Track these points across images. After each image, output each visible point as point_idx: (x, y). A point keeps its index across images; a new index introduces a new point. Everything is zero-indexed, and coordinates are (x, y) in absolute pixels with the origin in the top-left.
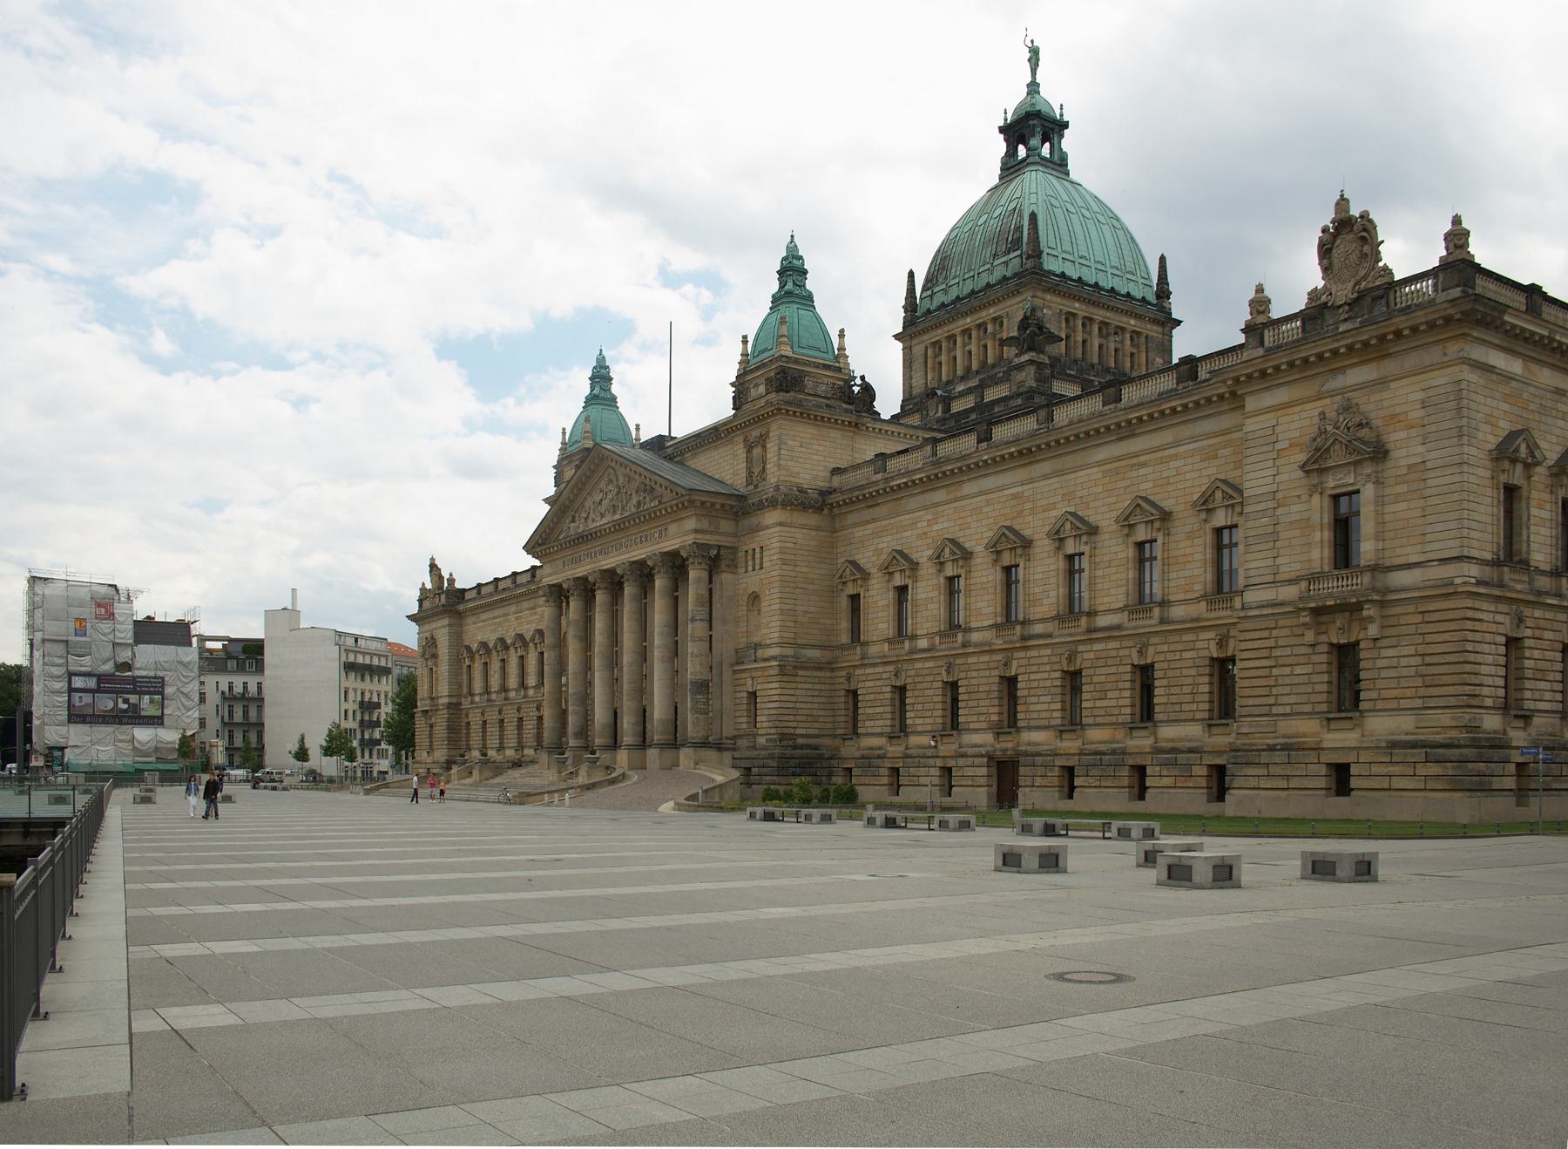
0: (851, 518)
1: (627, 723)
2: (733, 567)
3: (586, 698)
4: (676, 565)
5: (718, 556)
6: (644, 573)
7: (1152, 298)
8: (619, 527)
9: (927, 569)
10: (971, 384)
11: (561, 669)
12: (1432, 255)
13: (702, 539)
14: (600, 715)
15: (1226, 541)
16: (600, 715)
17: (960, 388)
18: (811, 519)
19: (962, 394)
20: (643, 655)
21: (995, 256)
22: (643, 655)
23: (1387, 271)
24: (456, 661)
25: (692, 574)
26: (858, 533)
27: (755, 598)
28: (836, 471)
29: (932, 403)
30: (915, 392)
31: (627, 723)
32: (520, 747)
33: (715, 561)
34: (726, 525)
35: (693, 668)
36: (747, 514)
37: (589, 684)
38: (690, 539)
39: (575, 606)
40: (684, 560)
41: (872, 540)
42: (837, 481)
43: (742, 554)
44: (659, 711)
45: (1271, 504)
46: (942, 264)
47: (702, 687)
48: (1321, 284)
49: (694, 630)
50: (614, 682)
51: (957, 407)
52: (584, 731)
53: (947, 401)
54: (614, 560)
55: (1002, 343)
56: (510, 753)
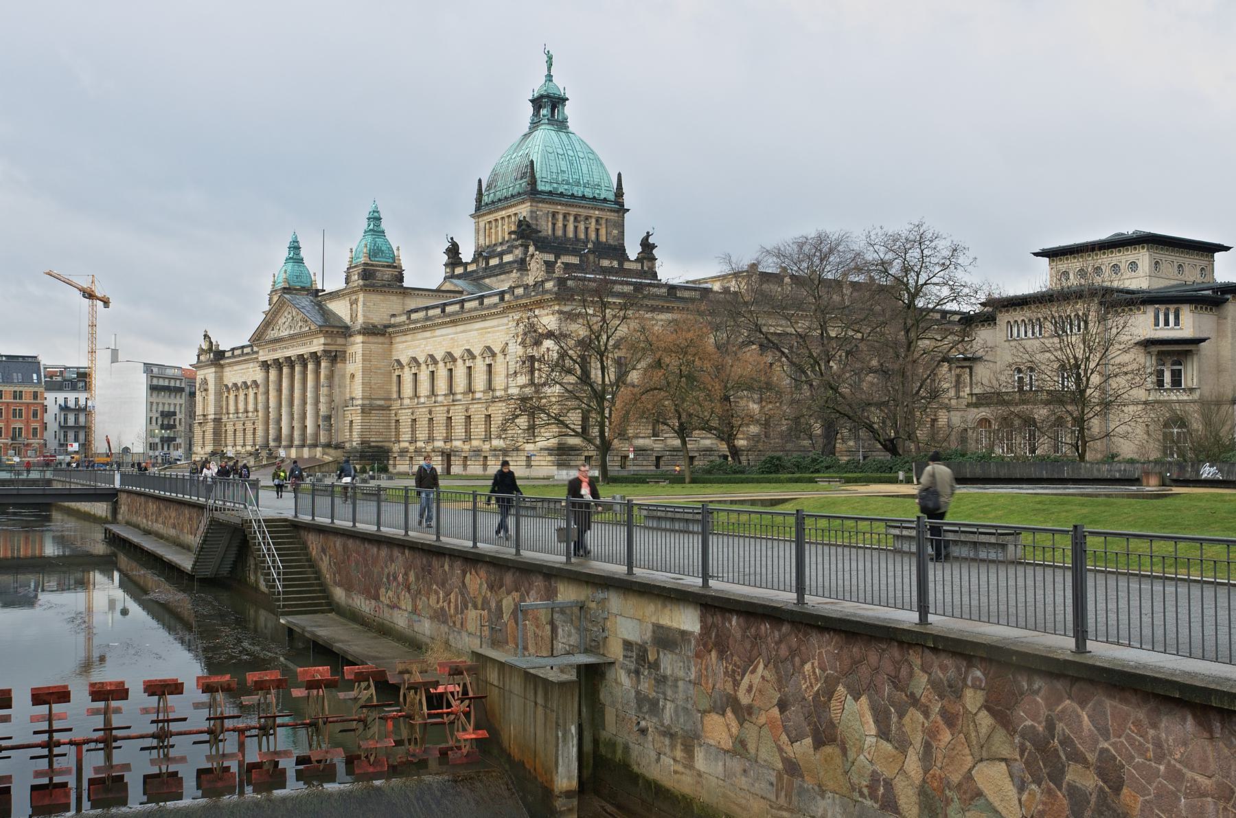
0: (398, 339)
2: (344, 360)
7: (612, 198)
8: (292, 337)
9: (441, 364)
13: (328, 348)
18: (381, 339)
22: (304, 403)
25: (323, 364)
26: (401, 346)
27: (353, 376)
28: (394, 315)
33: (335, 357)
34: (340, 341)
36: (350, 336)
38: (322, 348)
39: (273, 374)
41: (407, 348)
42: (393, 321)
47: (328, 418)
49: (323, 391)
54: (292, 352)
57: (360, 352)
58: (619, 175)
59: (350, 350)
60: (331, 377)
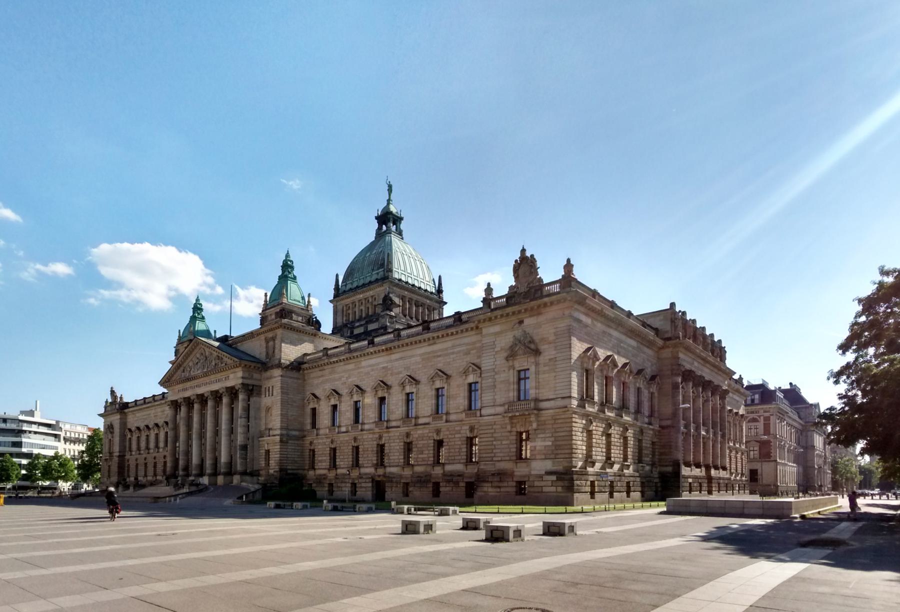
1: (208, 463)
2: (259, 394)
3: (188, 453)
4: (233, 393)
5: (252, 390)
6: (217, 396)
10: (363, 323)
11: (176, 438)
12: (559, 274)
14: (195, 460)
15: (473, 388)
16: (195, 460)
17: (357, 324)
19: (358, 327)
20: (217, 433)
21: (373, 270)
23: (540, 280)
24: (123, 436)
29: (345, 330)
30: (338, 325)
31: (208, 463)
32: (155, 475)
33: (252, 390)
35: (240, 439)
37: (189, 446)
40: (237, 391)
43: (263, 389)
44: (224, 458)
45: (493, 374)
46: (350, 272)
48: (514, 284)
49: (240, 422)
50: (202, 445)
51: (356, 332)
52: (186, 468)
53: (353, 328)
55: (375, 306)
56: (150, 478)
57: (279, 385)
58: (440, 277)
59: (267, 384)
60: (247, 409)
